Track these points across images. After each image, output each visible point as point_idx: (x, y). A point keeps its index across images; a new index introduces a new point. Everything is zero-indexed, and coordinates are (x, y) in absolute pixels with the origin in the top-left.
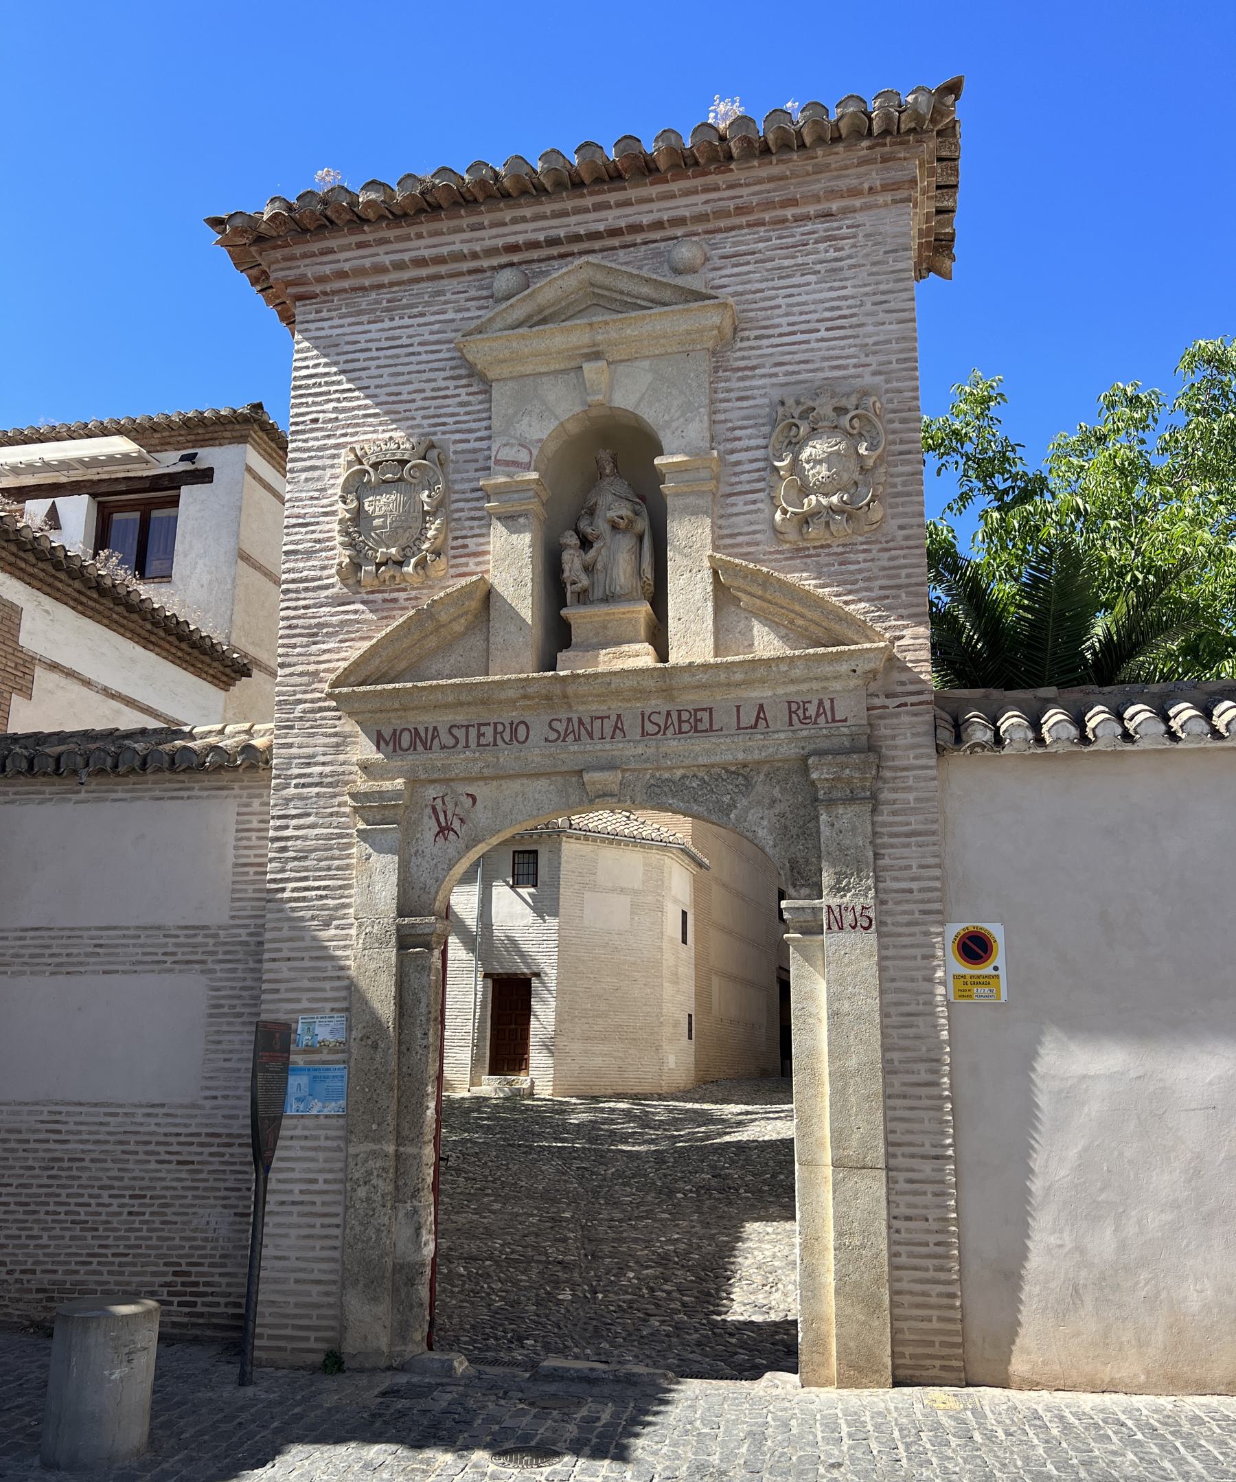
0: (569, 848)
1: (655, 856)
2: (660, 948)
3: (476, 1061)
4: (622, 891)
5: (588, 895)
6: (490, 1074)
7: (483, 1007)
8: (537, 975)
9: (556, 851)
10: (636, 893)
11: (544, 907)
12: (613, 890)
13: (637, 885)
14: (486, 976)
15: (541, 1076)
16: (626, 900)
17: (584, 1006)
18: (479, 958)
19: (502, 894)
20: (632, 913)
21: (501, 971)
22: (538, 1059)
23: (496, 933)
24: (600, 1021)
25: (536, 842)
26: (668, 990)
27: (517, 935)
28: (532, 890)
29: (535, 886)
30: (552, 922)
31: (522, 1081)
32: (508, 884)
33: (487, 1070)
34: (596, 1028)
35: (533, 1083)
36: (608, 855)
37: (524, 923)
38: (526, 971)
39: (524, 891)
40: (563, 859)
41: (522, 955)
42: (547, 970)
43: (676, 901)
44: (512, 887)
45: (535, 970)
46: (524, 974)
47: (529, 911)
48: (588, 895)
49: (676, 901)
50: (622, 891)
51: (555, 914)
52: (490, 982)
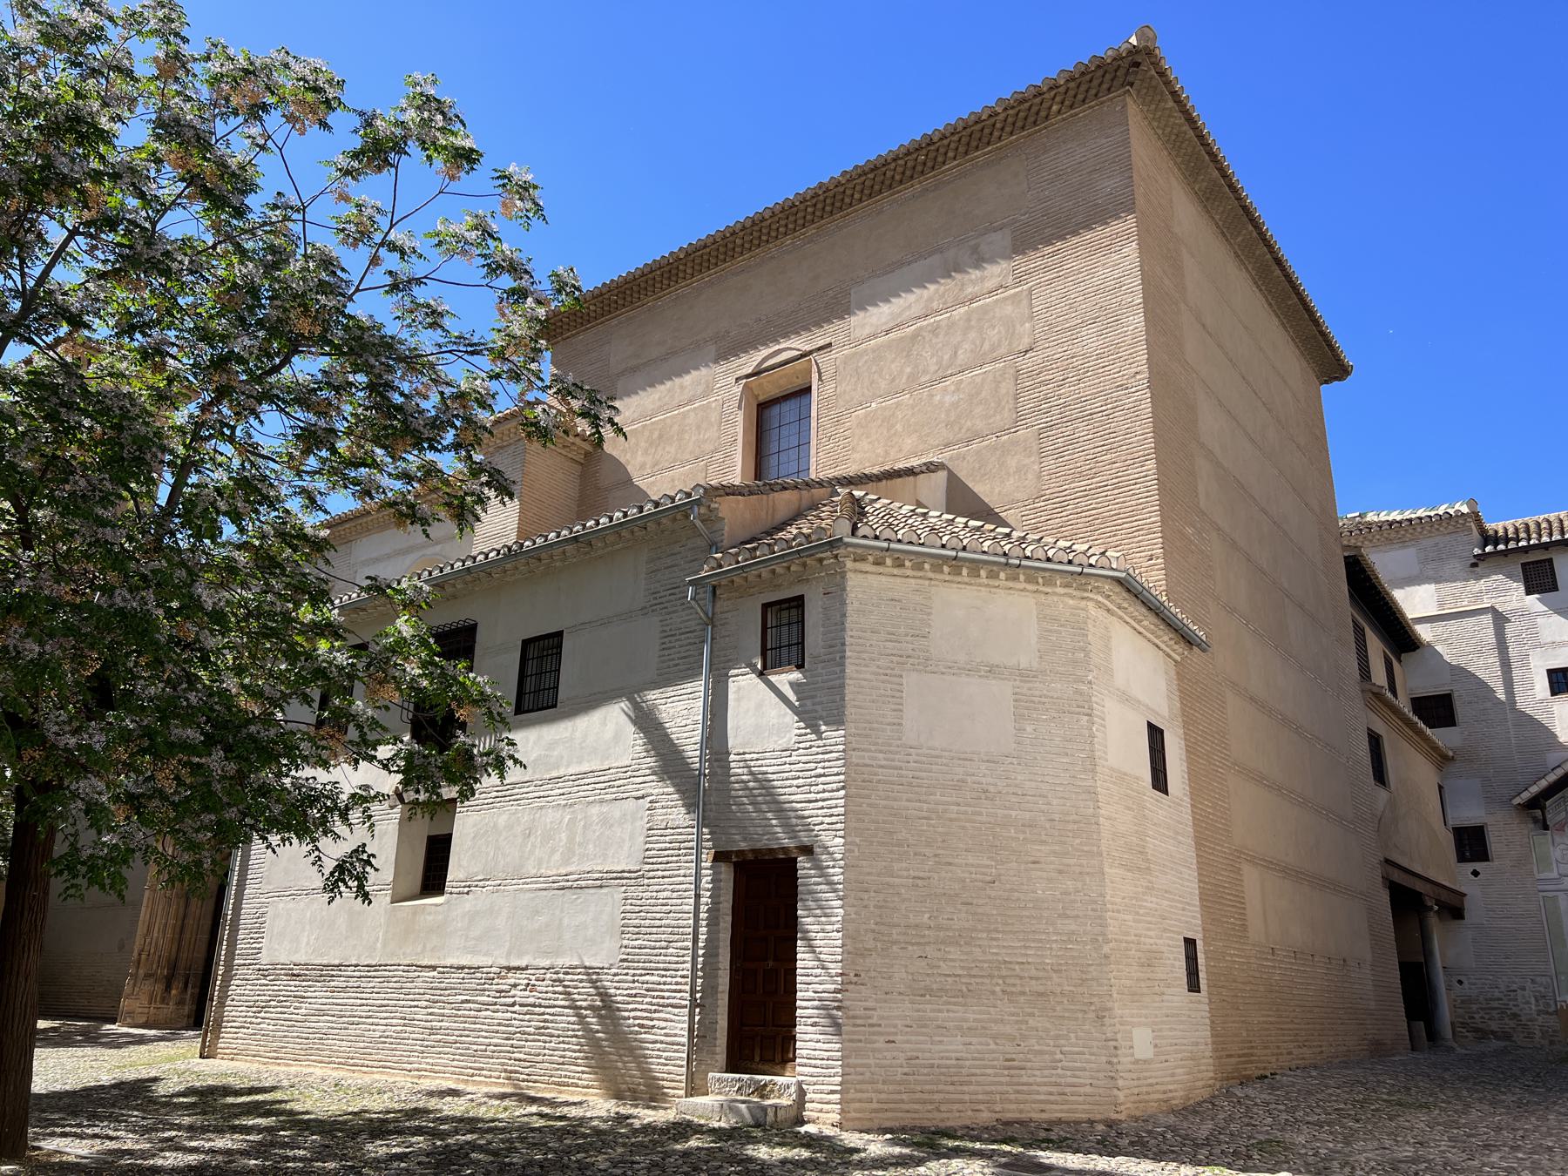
0: (865, 588)
1: (1063, 601)
2: (1092, 793)
3: (698, 1039)
4: (992, 670)
5: (911, 680)
6: (731, 1068)
7: (713, 922)
8: (808, 850)
9: (836, 592)
10: (1025, 675)
11: (818, 708)
12: (970, 670)
13: (1026, 660)
14: (719, 857)
15: (815, 1078)
16: (1003, 690)
17: (912, 919)
18: (704, 821)
19: (744, 687)
20: (1019, 717)
21: (743, 846)
22: (810, 1039)
23: (736, 769)
24: (954, 953)
25: (801, 581)
26: (1118, 885)
27: (769, 768)
28: (796, 675)
29: (800, 667)
30: (834, 736)
31: (782, 1087)
32: (752, 667)
33: (721, 1057)
34: (945, 968)
35: (801, 1093)
36: (955, 602)
37: (783, 743)
38: (786, 842)
39: (785, 679)
40: (850, 609)
41: (780, 809)
42: (826, 838)
43: (1126, 699)
44: (761, 674)
45: (806, 840)
46: (785, 850)
47: (790, 717)
48: (911, 680)
49: (1126, 699)
50: (992, 670)
51: (837, 720)
52: (727, 873)
